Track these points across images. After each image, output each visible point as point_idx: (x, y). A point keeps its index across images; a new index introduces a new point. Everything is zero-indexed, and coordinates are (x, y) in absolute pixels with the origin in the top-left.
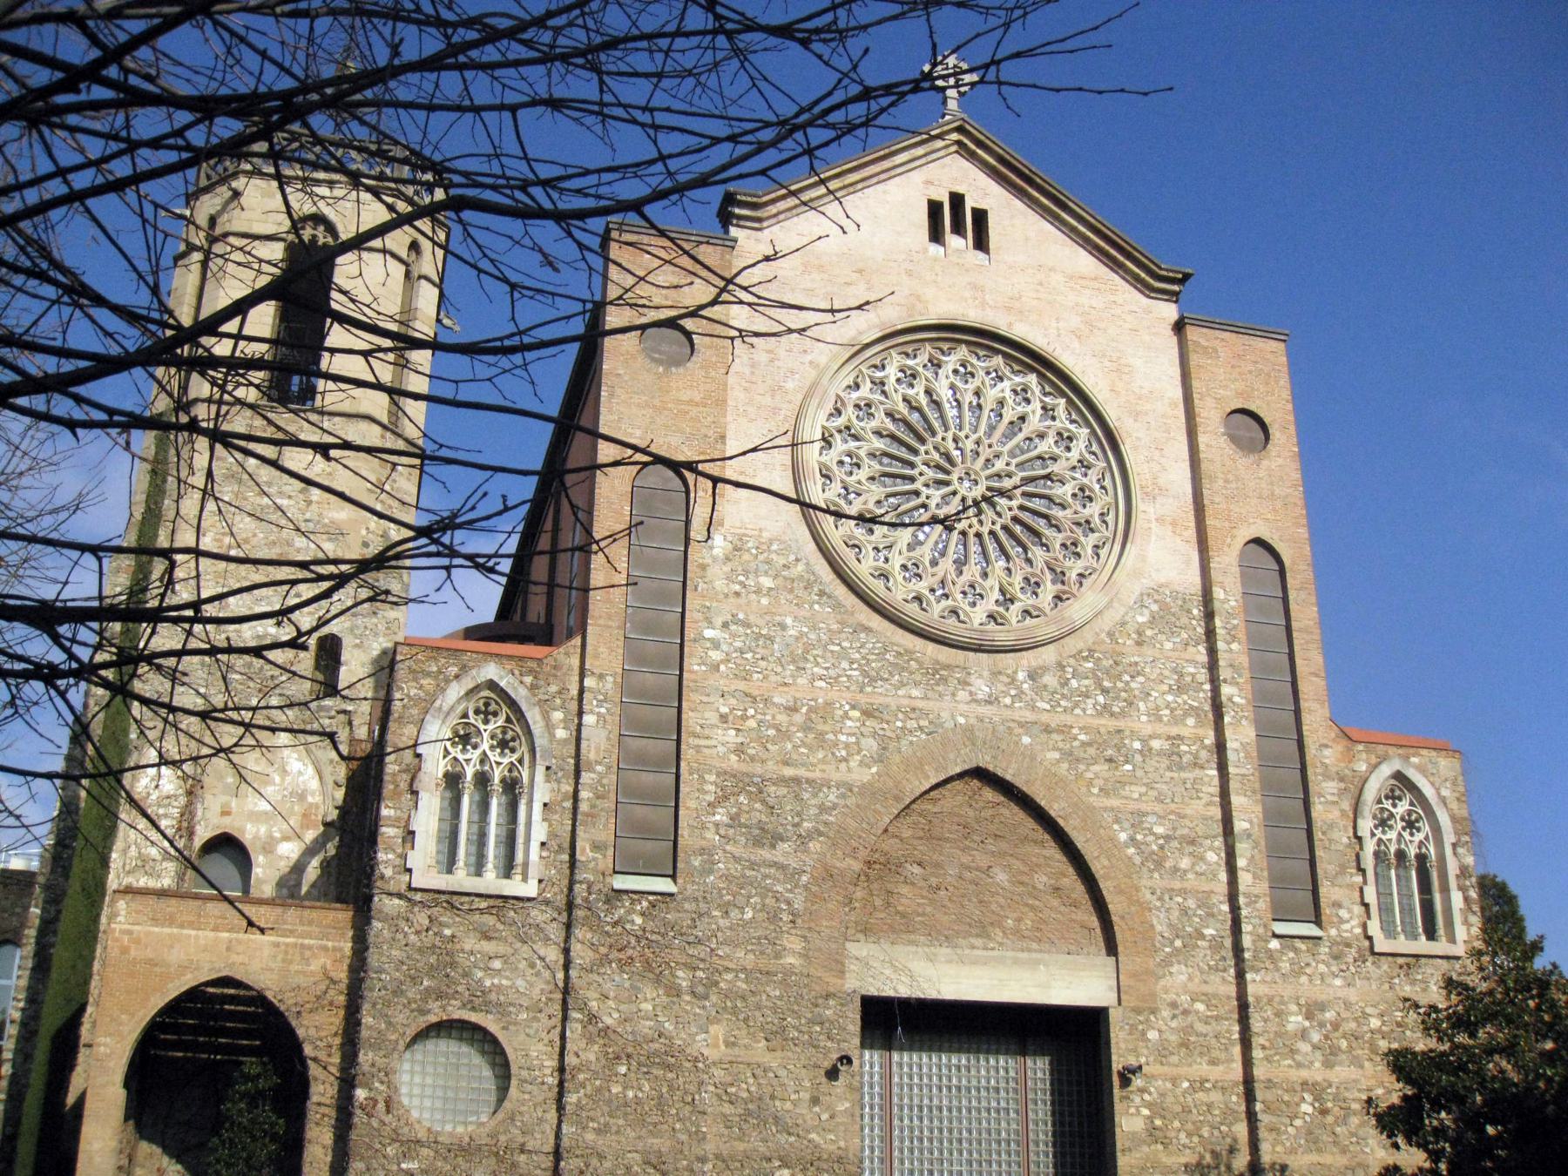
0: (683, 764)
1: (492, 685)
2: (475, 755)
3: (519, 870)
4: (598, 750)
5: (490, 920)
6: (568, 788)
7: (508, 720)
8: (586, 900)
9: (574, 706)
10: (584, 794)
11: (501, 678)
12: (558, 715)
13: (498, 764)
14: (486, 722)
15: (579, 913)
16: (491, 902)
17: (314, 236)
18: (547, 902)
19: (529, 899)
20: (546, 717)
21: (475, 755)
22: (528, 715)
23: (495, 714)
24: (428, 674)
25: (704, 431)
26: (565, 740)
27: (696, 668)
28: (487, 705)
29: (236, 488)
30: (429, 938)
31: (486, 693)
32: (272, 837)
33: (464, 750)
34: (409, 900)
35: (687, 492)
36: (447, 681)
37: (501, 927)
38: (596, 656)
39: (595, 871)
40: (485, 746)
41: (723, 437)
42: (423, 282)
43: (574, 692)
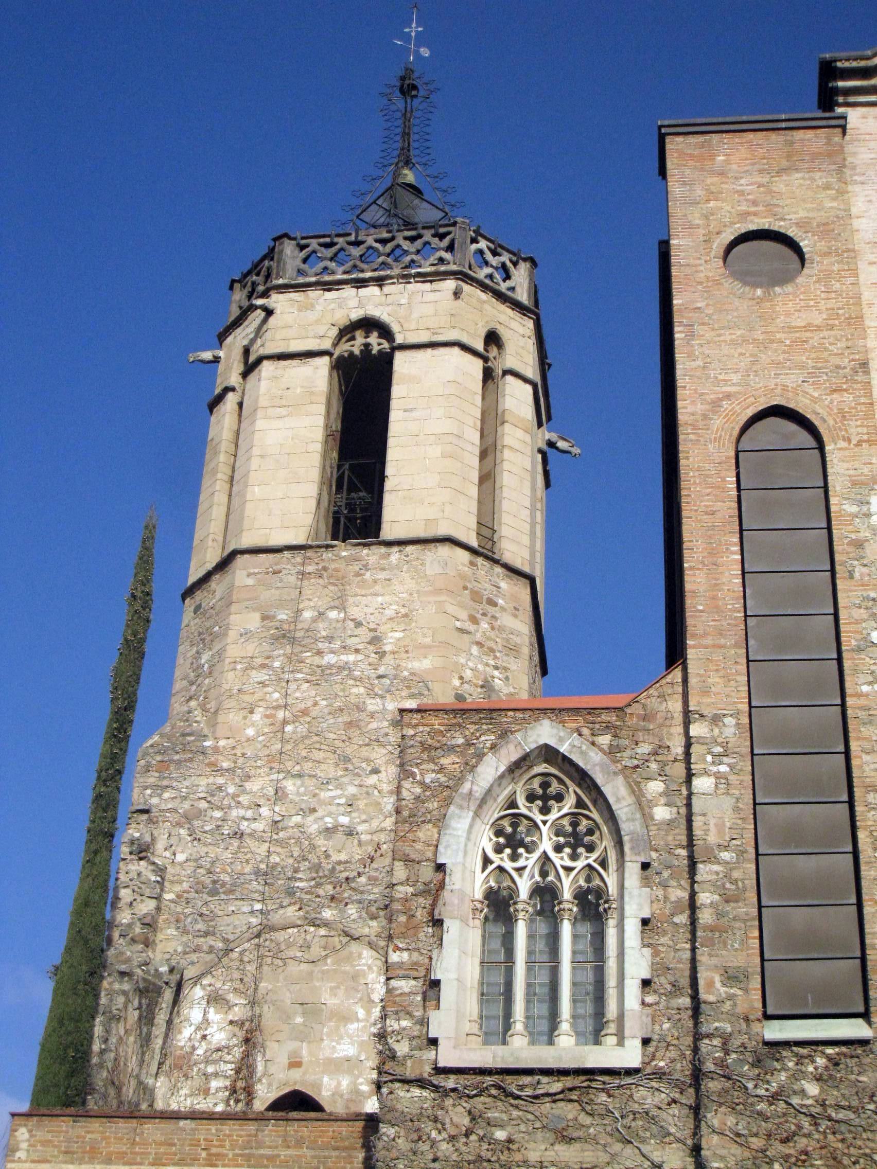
0: (862, 835)
1: (549, 753)
2: (530, 861)
3: (612, 1028)
4: (720, 827)
5: (568, 1111)
6: (679, 894)
7: (580, 804)
8: (721, 1063)
9: (679, 770)
10: (704, 898)
11: (561, 740)
12: (655, 787)
13: (568, 869)
14: (545, 810)
15: (712, 1086)
16: (569, 1081)
17: (367, 345)
18: (659, 1075)
19: (630, 1072)
20: (637, 792)
21: (530, 861)
22: (607, 790)
23: (559, 798)
24: (452, 749)
25: (836, 361)
26: (670, 823)
27: (865, 688)
28: (545, 785)
29: (288, 649)
30: (472, 1147)
31: (542, 768)
32: (357, 1092)
34: (436, 1088)
35: (821, 447)
36: (480, 756)
37: (587, 1120)
38: (706, 692)
39: (732, 1016)
40: (546, 845)
41: (864, 366)
42: (509, 378)
43: (678, 749)
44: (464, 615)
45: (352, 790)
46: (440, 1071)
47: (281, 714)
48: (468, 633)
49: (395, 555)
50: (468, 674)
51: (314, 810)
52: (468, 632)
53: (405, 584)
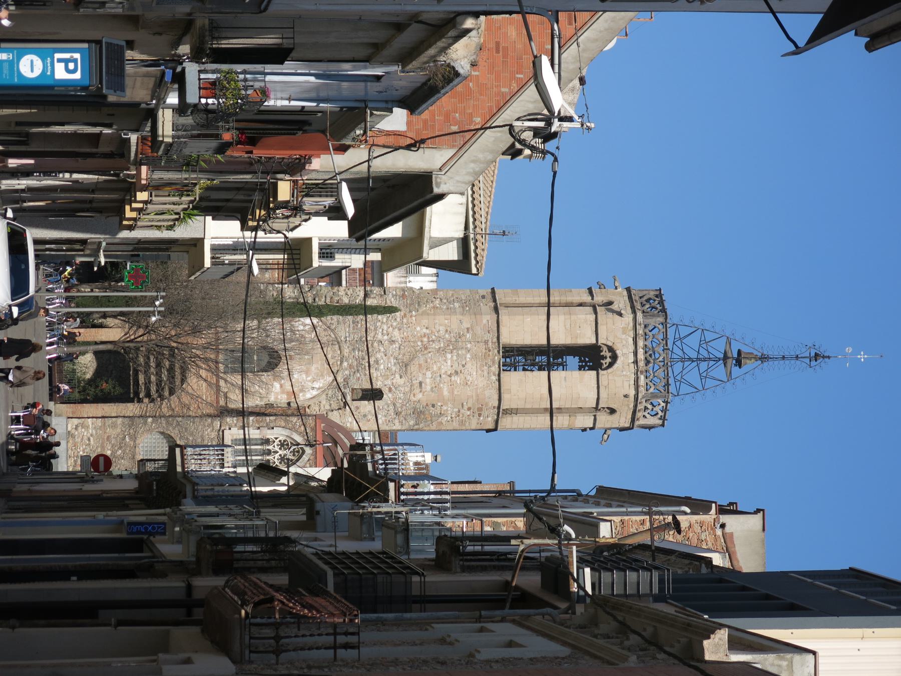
2: (277, 449)
13: (274, 458)
17: (606, 358)
21: (277, 449)
23: (294, 455)
33: (278, 445)
34: (219, 430)
40: (280, 452)
44: (470, 405)
45: (394, 368)
46: (223, 432)
47: (425, 339)
48: (463, 407)
49: (494, 378)
50: (445, 408)
51: (386, 355)
52: (463, 407)
53: (481, 382)
